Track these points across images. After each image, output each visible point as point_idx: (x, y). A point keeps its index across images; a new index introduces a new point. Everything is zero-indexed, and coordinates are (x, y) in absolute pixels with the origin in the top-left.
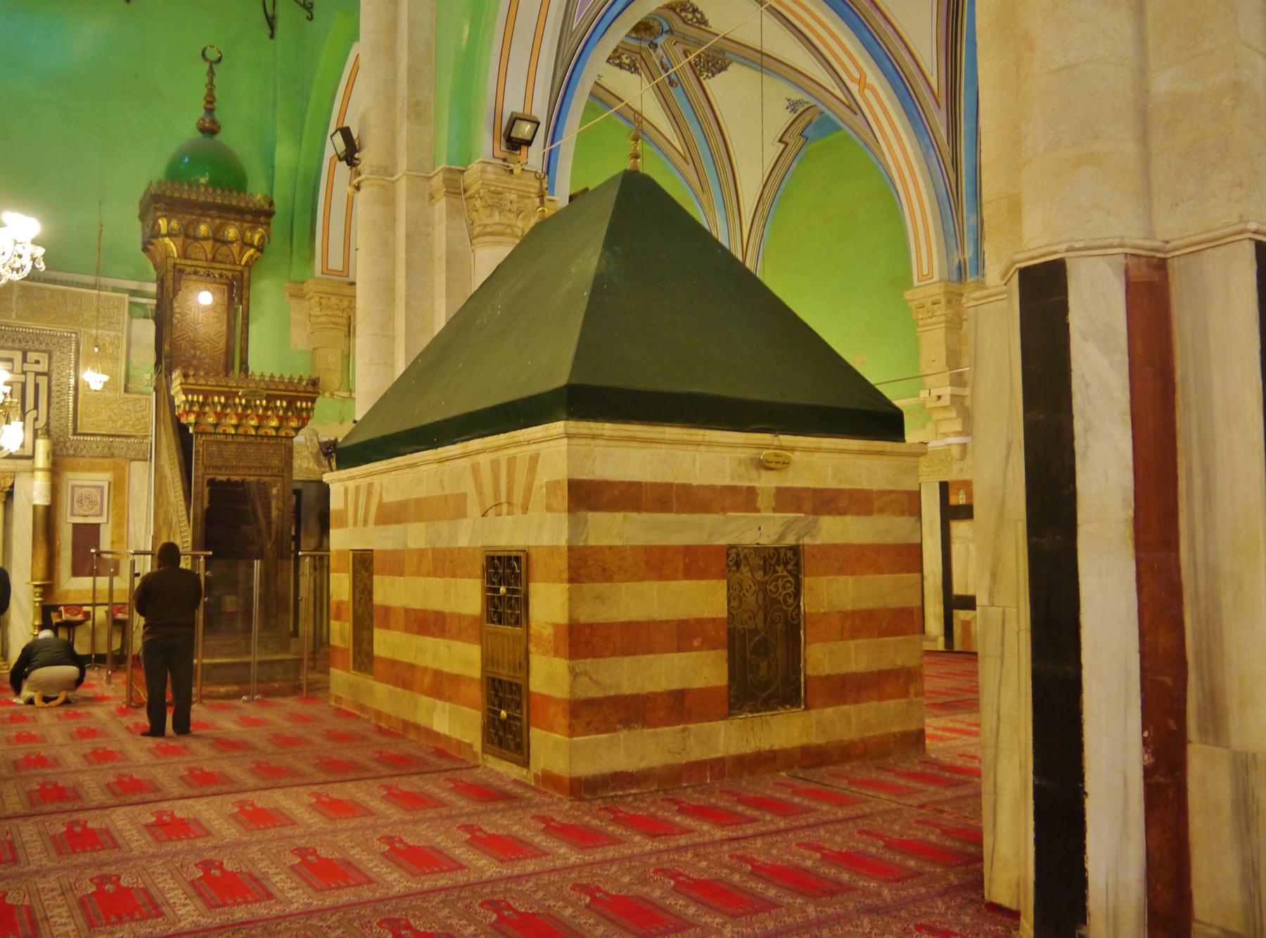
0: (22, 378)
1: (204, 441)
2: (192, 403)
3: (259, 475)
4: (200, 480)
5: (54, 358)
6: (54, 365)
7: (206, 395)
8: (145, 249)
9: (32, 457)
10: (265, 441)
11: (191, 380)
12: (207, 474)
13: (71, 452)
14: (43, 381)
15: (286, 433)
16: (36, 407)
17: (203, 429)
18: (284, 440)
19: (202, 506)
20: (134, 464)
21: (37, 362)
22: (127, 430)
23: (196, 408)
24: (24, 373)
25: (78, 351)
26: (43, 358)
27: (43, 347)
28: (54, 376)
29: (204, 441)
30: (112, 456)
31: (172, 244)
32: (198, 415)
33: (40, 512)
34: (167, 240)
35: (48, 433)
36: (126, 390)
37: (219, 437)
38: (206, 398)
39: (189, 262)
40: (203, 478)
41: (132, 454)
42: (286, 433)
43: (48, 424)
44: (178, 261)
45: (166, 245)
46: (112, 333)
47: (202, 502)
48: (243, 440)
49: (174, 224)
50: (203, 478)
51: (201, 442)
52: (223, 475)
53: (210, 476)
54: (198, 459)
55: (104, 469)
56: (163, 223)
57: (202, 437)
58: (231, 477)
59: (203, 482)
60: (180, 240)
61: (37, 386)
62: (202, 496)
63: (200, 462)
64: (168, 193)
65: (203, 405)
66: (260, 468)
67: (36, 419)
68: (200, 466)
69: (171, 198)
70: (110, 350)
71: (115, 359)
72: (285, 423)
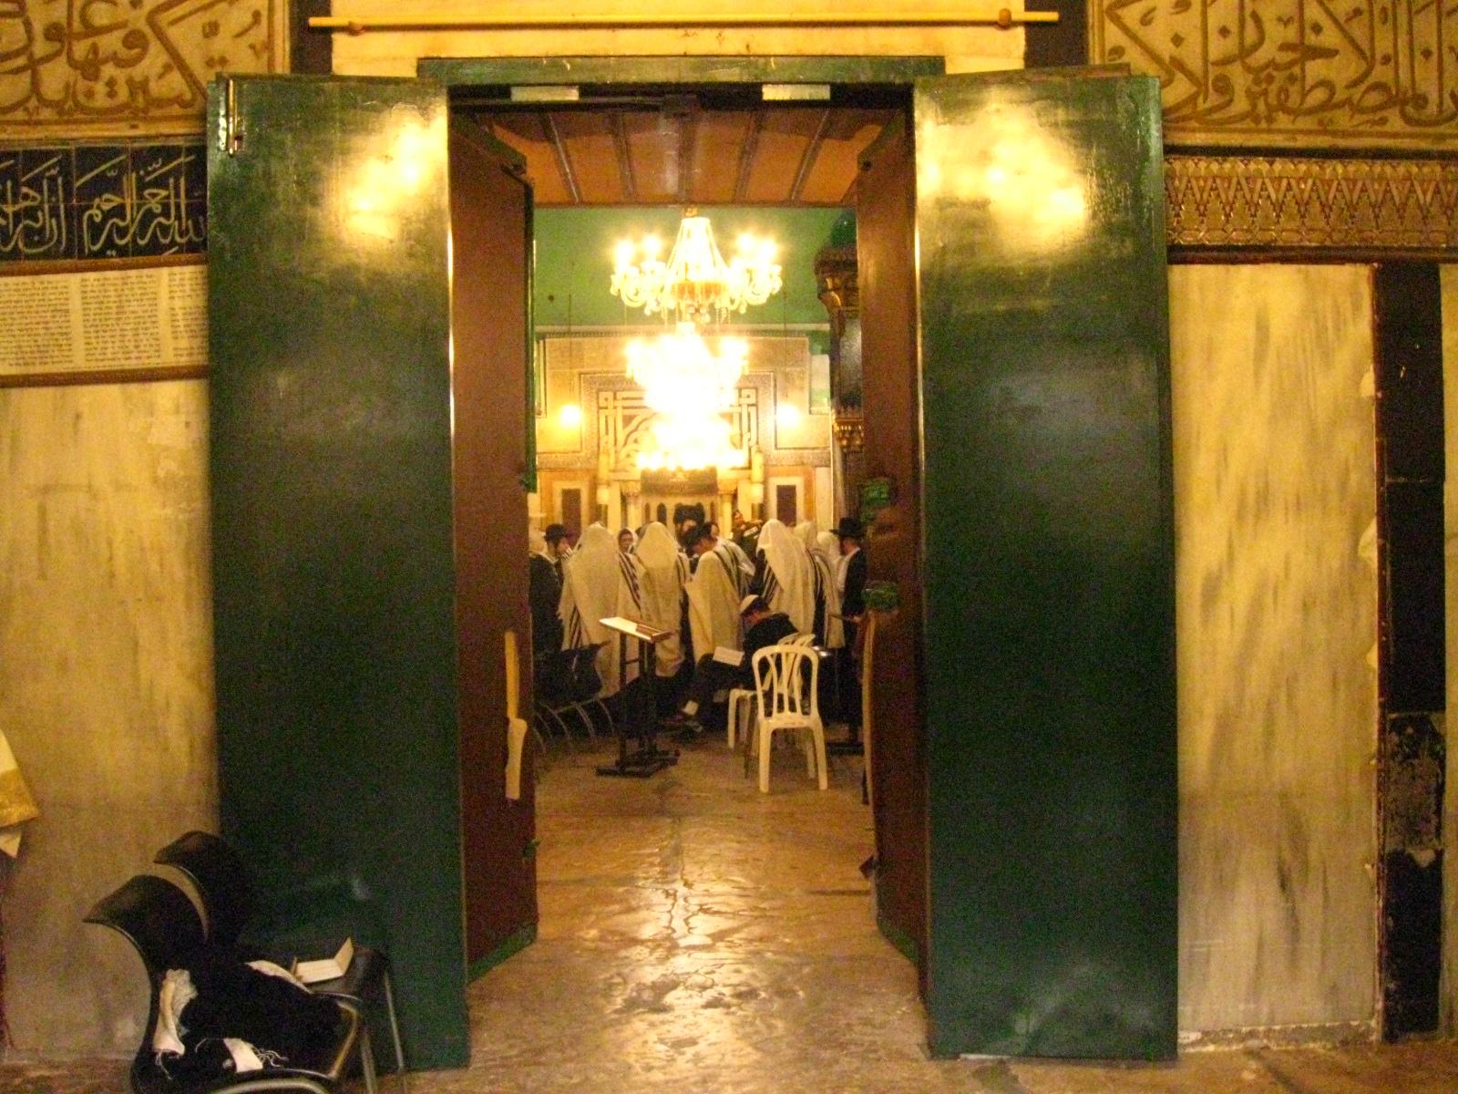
0: (739, 409)
2: (844, 432)
5: (760, 392)
6: (760, 398)
7: (854, 425)
8: (819, 297)
9: (750, 467)
11: (843, 415)
13: (774, 463)
14: (753, 410)
16: (749, 430)
20: (818, 469)
21: (748, 397)
22: (813, 444)
23: (847, 435)
24: (740, 405)
25: (775, 386)
26: (752, 393)
27: (752, 385)
28: (760, 406)
30: (803, 464)
31: (837, 297)
32: (848, 440)
33: (757, 508)
34: (833, 293)
35: (760, 451)
36: (810, 412)
38: (853, 426)
39: (850, 308)
41: (816, 462)
43: (757, 443)
44: (842, 309)
45: (833, 298)
46: (798, 369)
49: (837, 281)
55: (796, 474)
56: (829, 281)
60: (842, 293)
61: (749, 416)
64: (832, 257)
65: (851, 432)
67: (749, 440)
69: (834, 261)
70: (797, 382)
71: (802, 389)
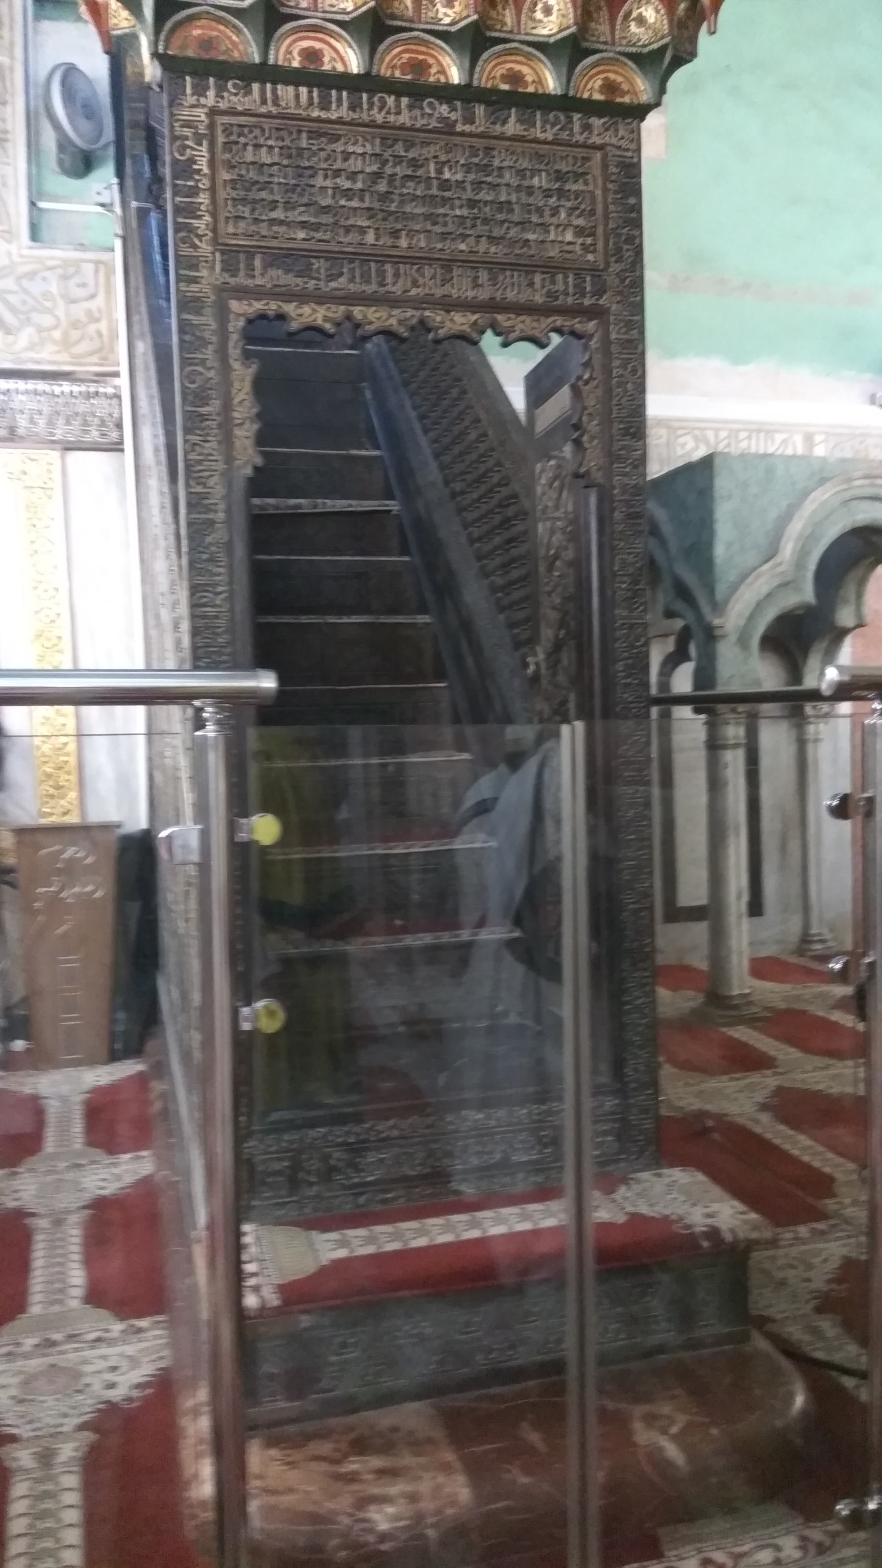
1: (213, 112)
3: (493, 306)
4: (208, 320)
10: (512, 127)
12: (242, 293)
15: (610, 87)
17: (207, 43)
18: (597, 122)
19: (229, 459)
29: (213, 112)
37: (286, 92)
40: (223, 314)
42: (610, 87)
47: (227, 441)
48: (404, 118)
50: (223, 314)
51: (201, 115)
52: (321, 299)
53: (258, 306)
54: (190, 211)
57: (200, 90)
58: (357, 312)
59: (223, 333)
62: (227, 407)
63: (202, 224)
66: (495, 267)
68: (205, 248)
72: (602, 28)
